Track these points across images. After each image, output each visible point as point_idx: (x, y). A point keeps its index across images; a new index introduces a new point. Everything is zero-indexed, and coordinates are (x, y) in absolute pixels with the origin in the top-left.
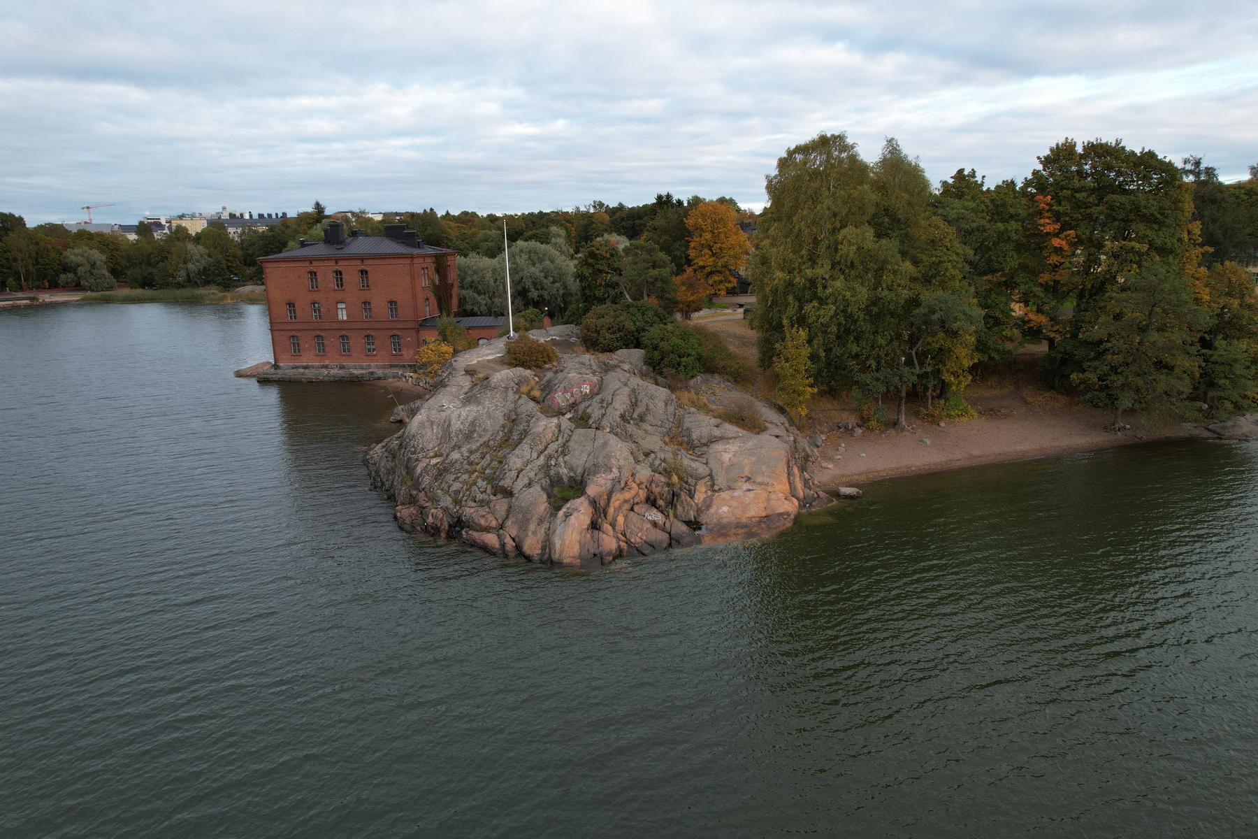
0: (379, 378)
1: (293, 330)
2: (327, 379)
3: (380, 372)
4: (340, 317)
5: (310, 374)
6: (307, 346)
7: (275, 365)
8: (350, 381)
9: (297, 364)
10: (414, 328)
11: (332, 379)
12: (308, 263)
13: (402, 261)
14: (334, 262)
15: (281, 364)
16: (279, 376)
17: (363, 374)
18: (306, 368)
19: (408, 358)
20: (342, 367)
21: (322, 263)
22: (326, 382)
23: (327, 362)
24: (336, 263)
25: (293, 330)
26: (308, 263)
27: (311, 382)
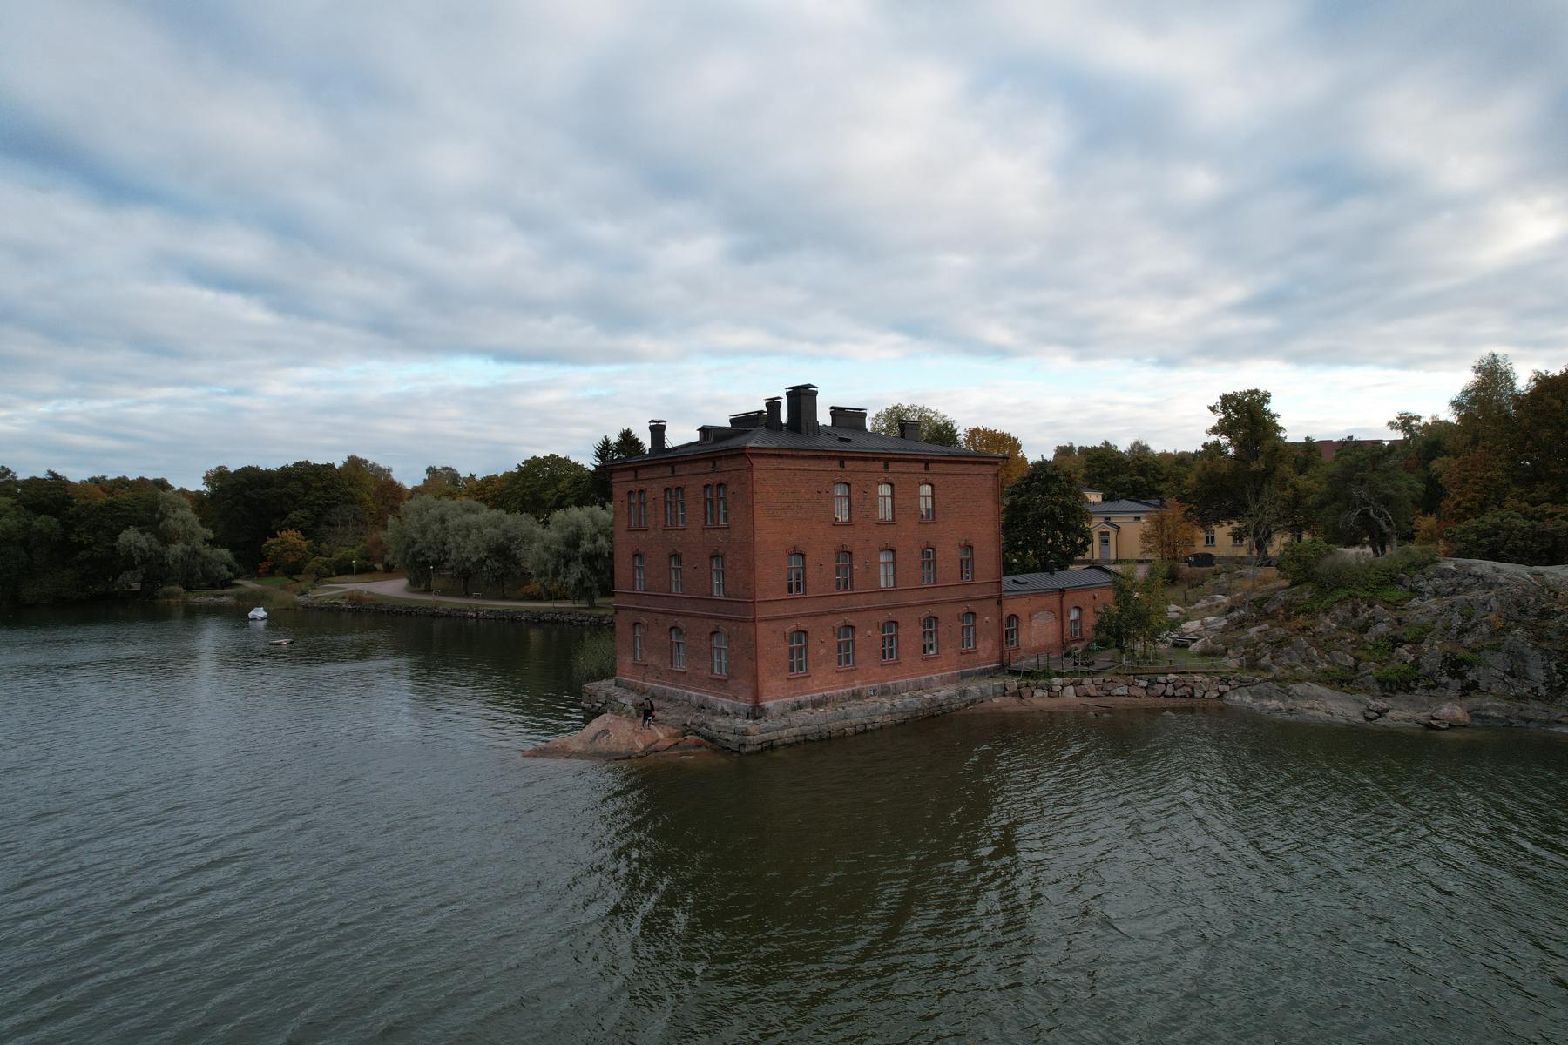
0: (973, 702)
1: (796, 617)
2: (888, 720)
3: (974, 688)
4: (883, 585)
5: (857, 714)
6: (822, 651)
7: (754, 709)
8: (928, 718)
9: (802, 698)
10: (992, 598)
11: (898, 718)
12: (836, 463)
13: (983, 469)
14: (883, 463)
15: (769, 704)
16: (796, 731)
17: (949, 698)
18: (816, 704)
19: (985, 656)
20: (885, 692)
21: (860, 465)
22: (891, 727)
23: (857, 686)
24: (886, 467)
25: (796, 617)
26: (836, 463)
27: (866, 731)
